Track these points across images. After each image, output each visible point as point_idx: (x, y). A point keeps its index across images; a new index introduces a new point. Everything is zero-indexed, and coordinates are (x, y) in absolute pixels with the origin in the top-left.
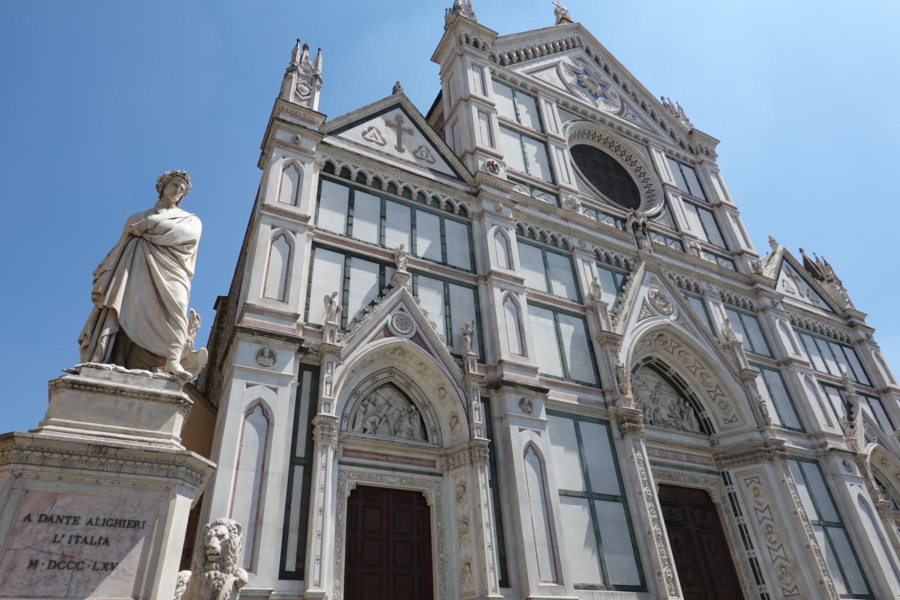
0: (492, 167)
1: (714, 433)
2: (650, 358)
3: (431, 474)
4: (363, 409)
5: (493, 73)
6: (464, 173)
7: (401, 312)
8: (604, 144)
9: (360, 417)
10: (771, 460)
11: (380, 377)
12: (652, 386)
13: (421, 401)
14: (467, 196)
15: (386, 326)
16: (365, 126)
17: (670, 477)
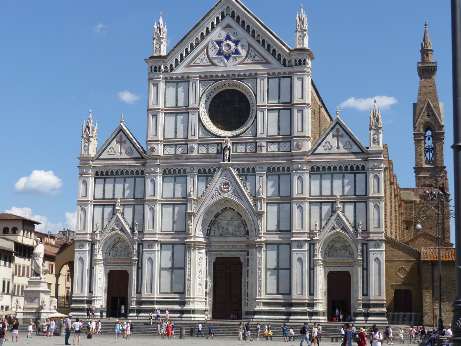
0: (152, 149)
1: (248, 235)
2: (226, 208)
3: (128, 266)
4: (112, 250)
5: (166, 78)
6: (143, 155)
7: (118, 222)
8: (233, 86)
9: (111, 252)
10: (256, 248)
11: (116, 240)
12: (229, 218)
13: (128, 245)
14: (143, 166)
15: (113, 228)
16: (108, 149)
17: (222, 255)
